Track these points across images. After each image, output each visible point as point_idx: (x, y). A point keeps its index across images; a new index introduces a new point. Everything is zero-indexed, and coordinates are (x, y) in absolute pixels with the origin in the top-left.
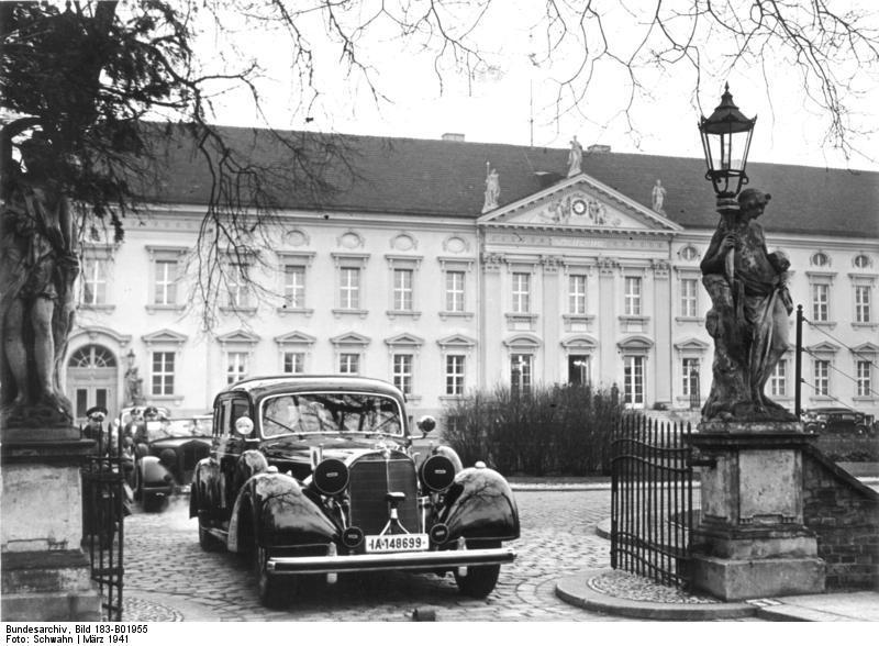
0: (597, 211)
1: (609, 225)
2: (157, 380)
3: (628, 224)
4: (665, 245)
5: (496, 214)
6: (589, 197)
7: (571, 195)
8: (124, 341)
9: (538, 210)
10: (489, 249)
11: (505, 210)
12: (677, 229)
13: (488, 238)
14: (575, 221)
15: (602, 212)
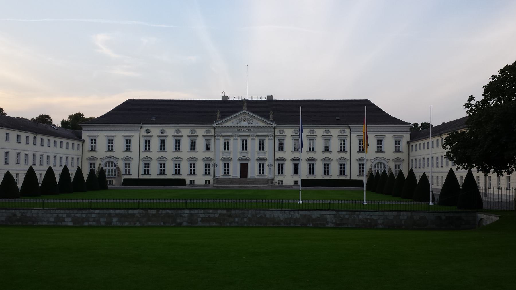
0: (250, 120)
1: (254, 124)
2: (126, 170)
3: (260, 123)
4: (273, 130)
5: (218, 123)
6: (246, 115)
7: (242, 116)
8: (117, 159)
9: (232, 121)
10: (217, 133)
11: (221, 122)
12: (274, 125)
13: (216, 130)
14: (243, 123)
15: (251, 120)
